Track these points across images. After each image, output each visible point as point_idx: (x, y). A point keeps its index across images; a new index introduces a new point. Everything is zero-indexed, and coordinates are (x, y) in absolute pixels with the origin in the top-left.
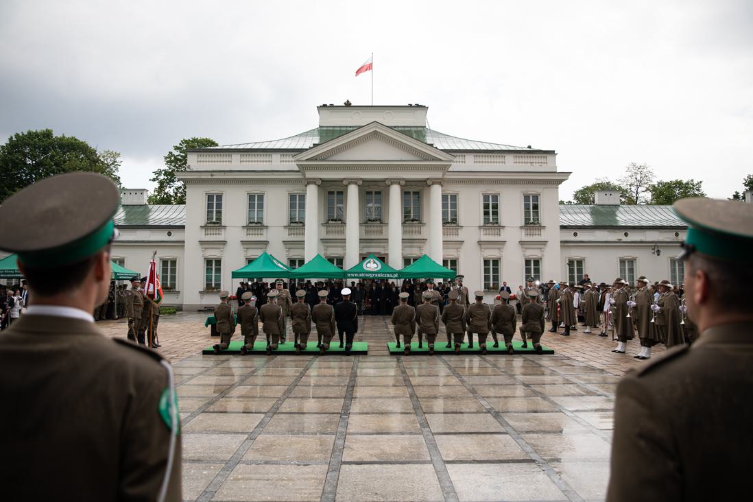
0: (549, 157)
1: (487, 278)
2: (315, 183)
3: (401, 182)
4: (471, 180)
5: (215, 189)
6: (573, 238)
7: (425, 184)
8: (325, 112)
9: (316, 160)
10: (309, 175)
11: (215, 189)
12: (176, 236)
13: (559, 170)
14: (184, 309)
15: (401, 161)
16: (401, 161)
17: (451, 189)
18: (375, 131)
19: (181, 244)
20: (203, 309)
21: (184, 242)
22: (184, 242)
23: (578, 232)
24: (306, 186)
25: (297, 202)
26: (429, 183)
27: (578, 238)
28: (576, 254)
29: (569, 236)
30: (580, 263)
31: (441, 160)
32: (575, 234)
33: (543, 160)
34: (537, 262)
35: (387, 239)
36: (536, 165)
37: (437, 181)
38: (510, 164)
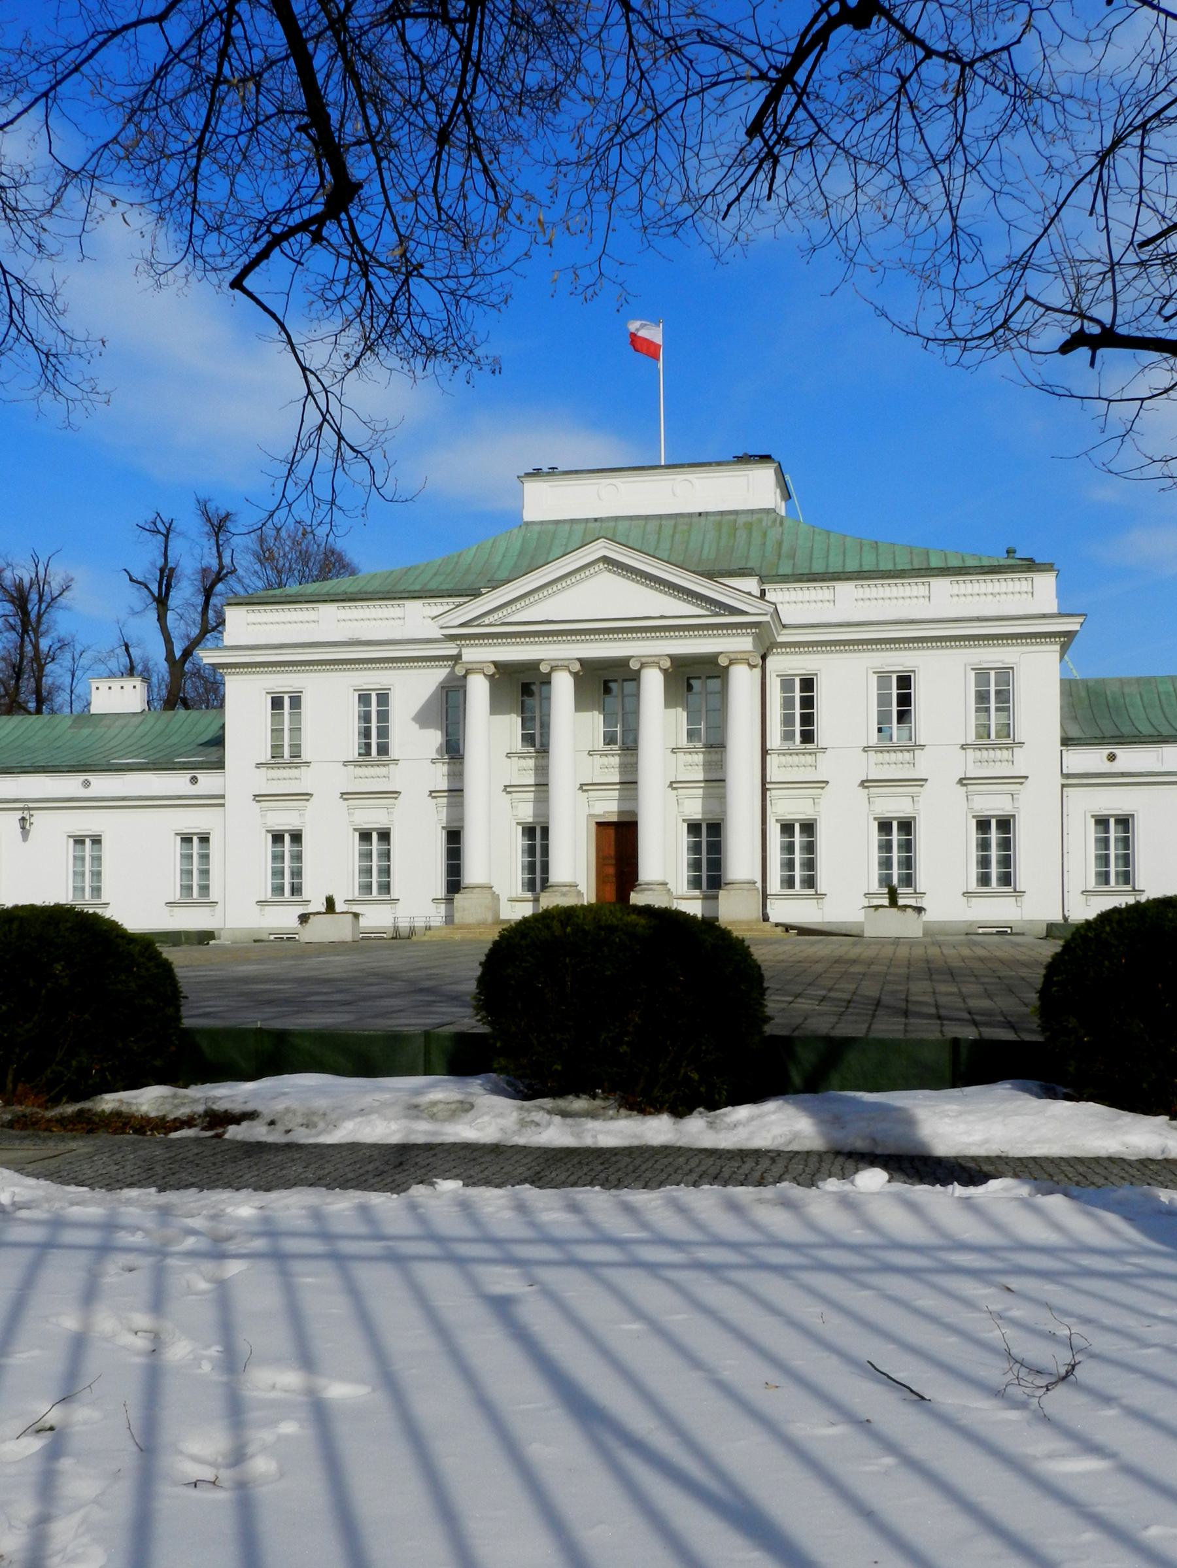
1: (886, 863)
3: (661, 662)
5: (284, 682)
6: (1107, 767)
12: (208, 782)
15: (662, 617)
16: (662, 617)
19: (217, 800)
22: (223, 797)
23: (1120, 752)
26: (722, 661)
27: (1121, 765)
28: (1113, 801)
29: (1090, 759)
30: (1124, 822)
32: (1112, 757)
33: (1025, 586)
34: (1005, 824)
35: (724, 781)
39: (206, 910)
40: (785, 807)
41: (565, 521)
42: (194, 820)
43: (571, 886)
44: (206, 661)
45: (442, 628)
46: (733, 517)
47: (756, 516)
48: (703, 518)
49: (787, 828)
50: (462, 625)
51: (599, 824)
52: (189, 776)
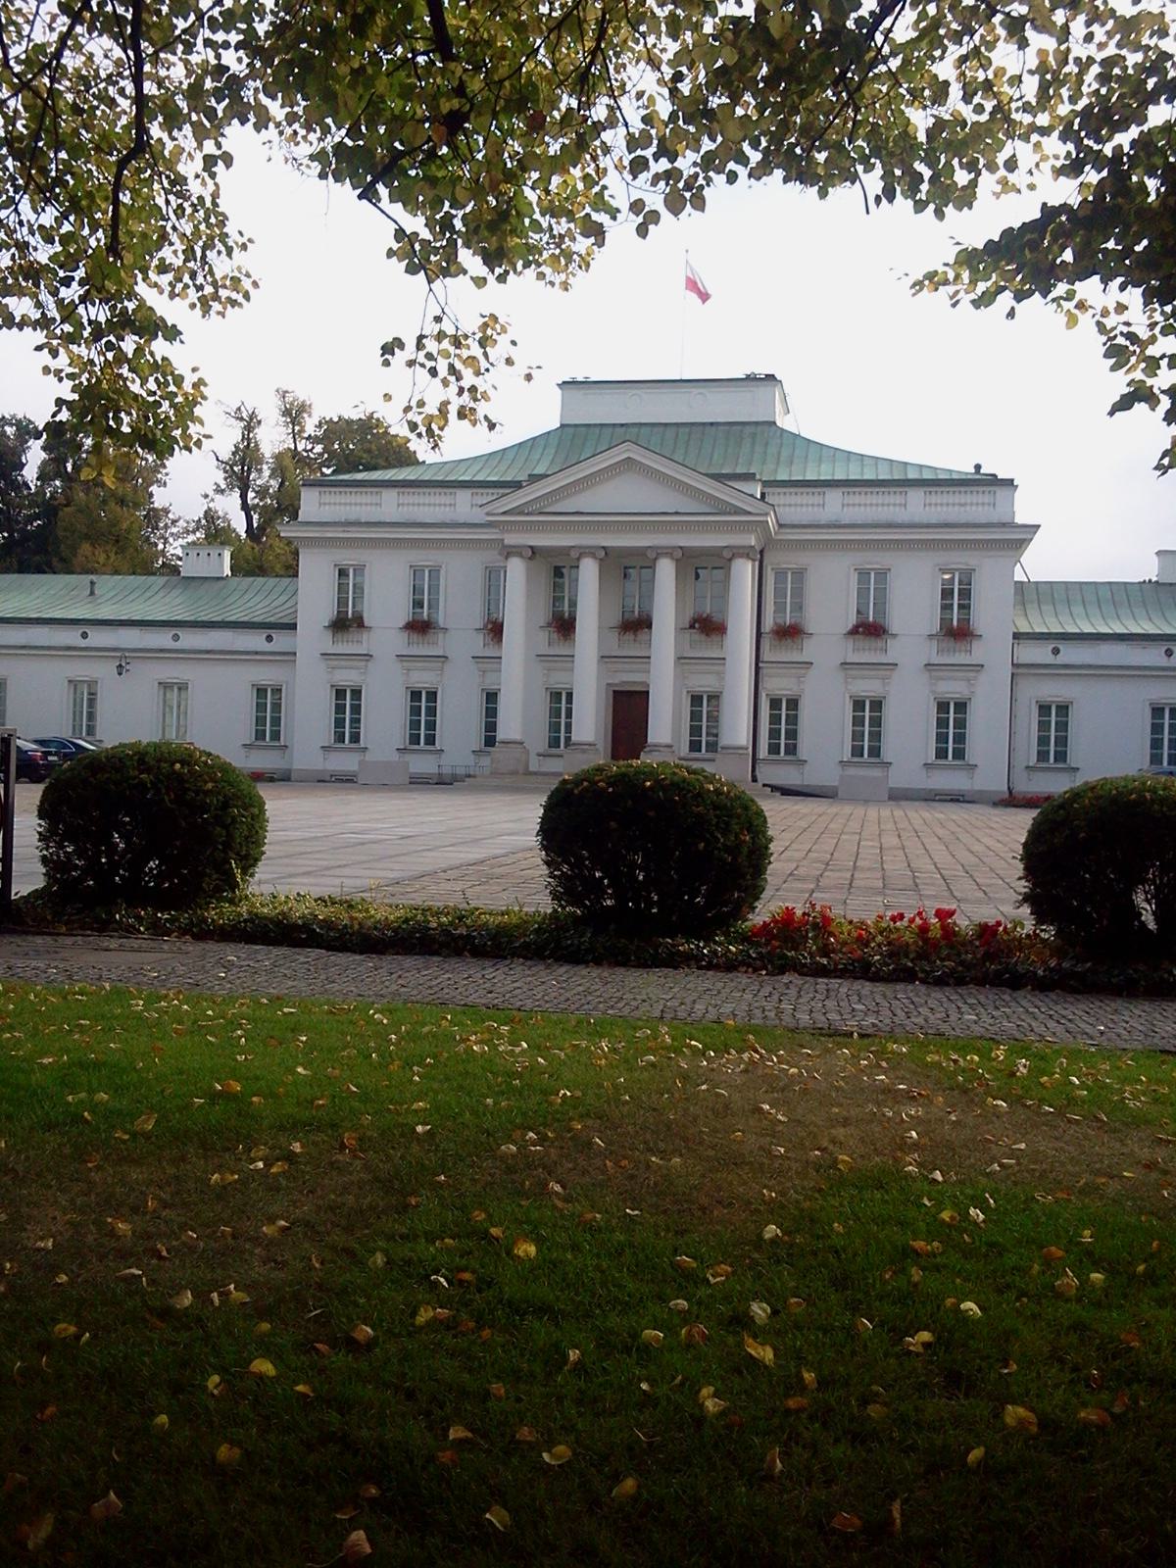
0: (1001, 493)
2: (521, 555)
4: (836, 539)
7: (720, 561)
8: (577, 394)
9: (521, 513)
10: (511, 539)
11: (348, 557)
12: (281, 641)
13: (1019, 520)
14: (294, 776)
15: (677, 513)
16: (677, 513)
17: (790, 560)
18: (629, 458)
20: (328, 778)
21: (295, 654)
24: (506, 558)
25: (493, 581)
31: (750, 513)
36: (972, 507)
37: (741, 551)
38: (916, 506)
39: (276, 753)
40: (778, 684)
41: (595, 425)
42: (267, 675)
43: (590, 745)
44: (282, 535)
45: (488, 514)
46: (739, 428)
47: (760, 428)
48: (714, 428)
49: (775, 703)
50: (504, 513)
51: (614, 692)
52: (265, 636)
